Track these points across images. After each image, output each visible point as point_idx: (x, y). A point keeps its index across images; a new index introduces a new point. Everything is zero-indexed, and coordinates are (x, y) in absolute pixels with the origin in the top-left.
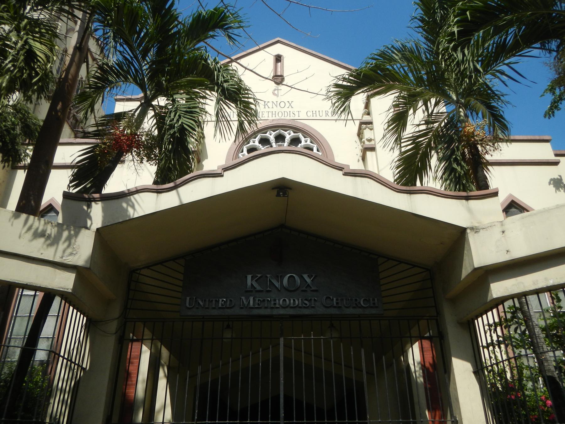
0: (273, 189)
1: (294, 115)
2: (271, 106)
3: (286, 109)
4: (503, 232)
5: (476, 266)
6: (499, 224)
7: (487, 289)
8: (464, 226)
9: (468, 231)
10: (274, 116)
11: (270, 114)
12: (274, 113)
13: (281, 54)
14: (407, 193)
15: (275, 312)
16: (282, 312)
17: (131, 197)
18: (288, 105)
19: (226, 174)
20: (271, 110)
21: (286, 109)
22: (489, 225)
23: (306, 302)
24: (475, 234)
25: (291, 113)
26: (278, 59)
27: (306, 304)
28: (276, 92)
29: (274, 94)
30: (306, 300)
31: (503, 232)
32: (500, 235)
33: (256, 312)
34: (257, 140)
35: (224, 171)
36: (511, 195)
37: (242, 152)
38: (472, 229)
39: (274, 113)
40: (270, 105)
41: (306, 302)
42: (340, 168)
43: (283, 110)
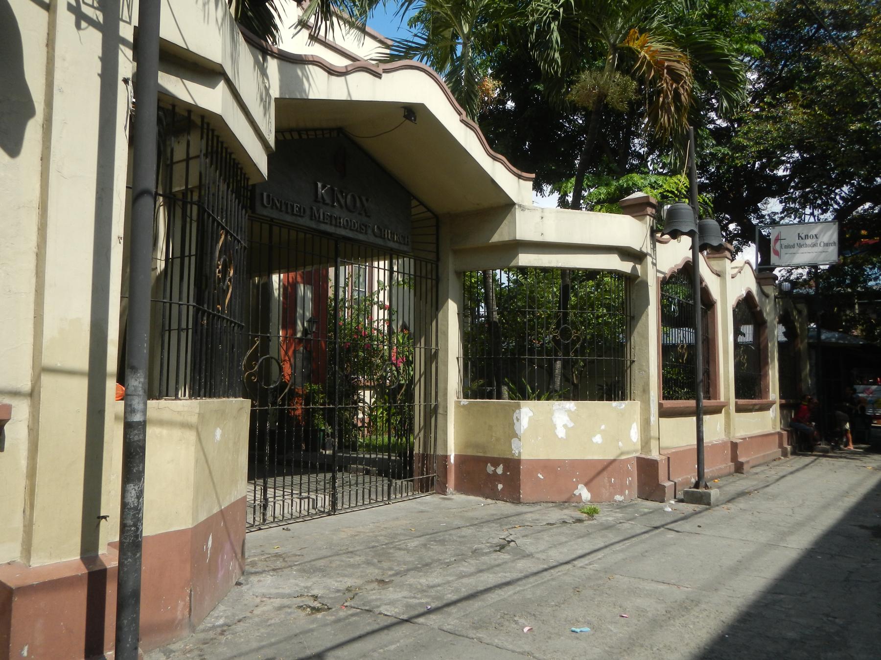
0: (403, 107)
4: (542, 218)
5: (518, 237)
6: (540, 211)
7: (515, 256)
8: (515, 202)
9: (517, 207)
14: (493, 158)
17: (306, 66)
19: (384, 75)
22: (533, 208)
23: (363, 227)
24: (522, 212)
27: (363, 230)
30: (363, 225)
31: (542, 218)
32: (539, 219)
35: (383, 72)
38: (520, 206)
41: (363, 227)
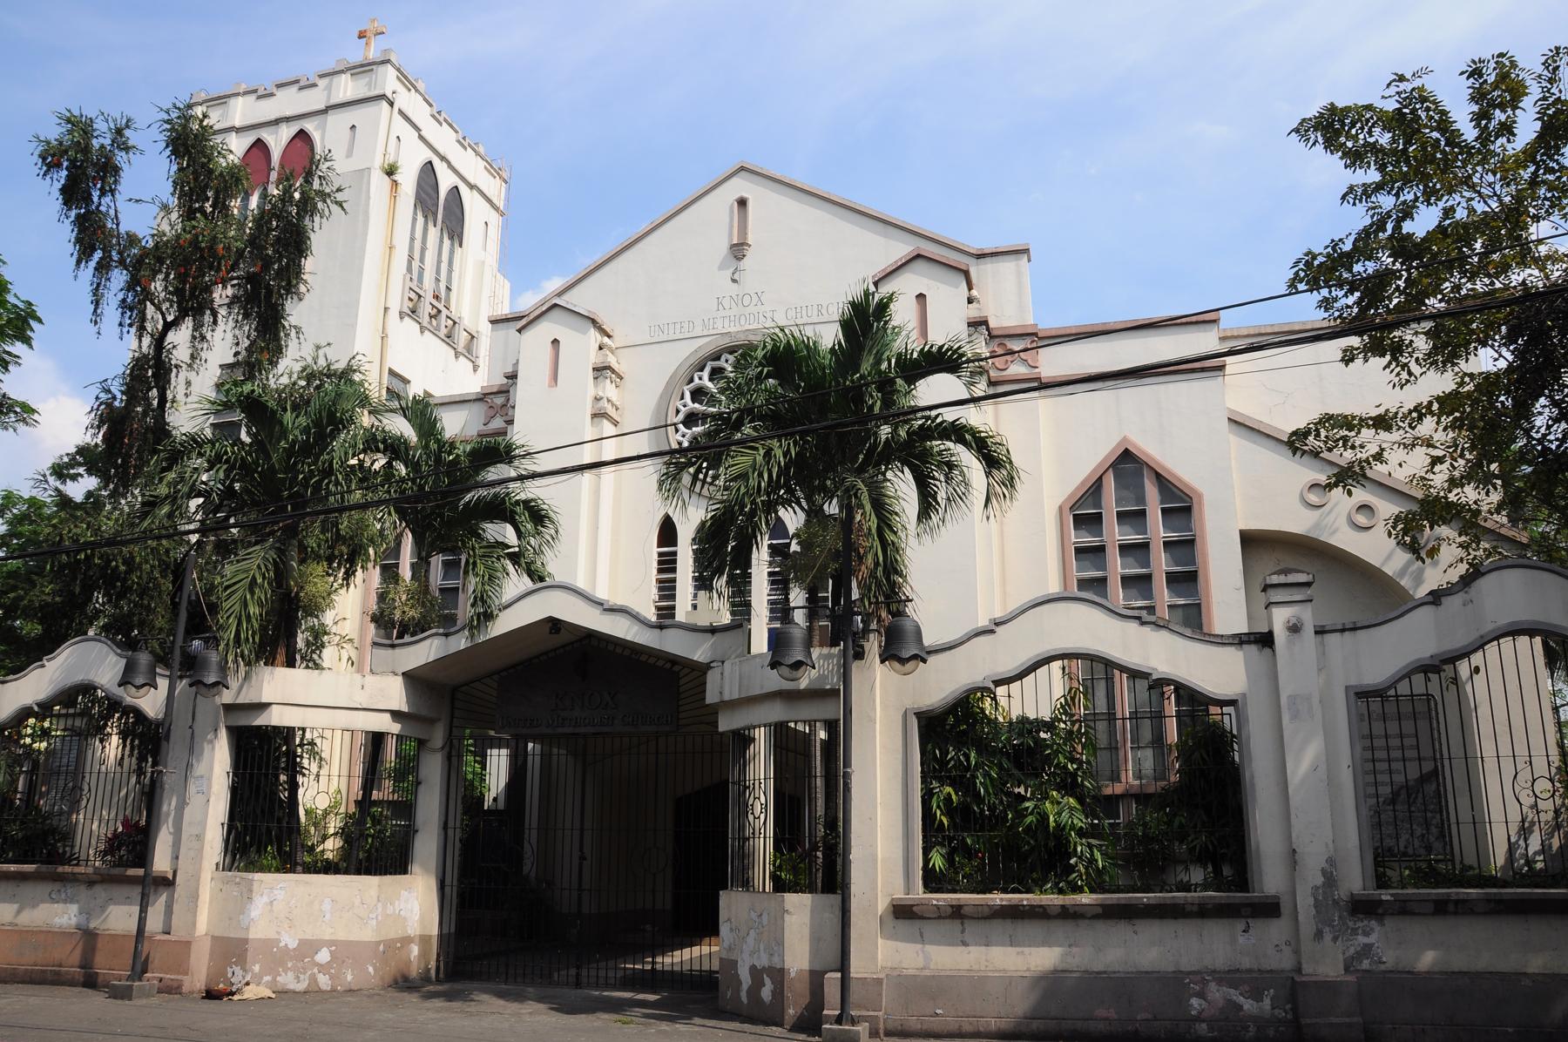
1: (764, 320)
2: (727, 307)
3: (752, 309)
10: (732, 324)
11: (727, 320)
12: (732, 318)
13: (745, 195)
15: (577, 730)
16: (582, 730)
18: (755, 298)
20: (727, 313)
21: (752, 309)
25: (761, 315)
26: (742, 203)
28: (736, 277)
29: (734, 281)
33: (560, 730)
34: (706, 374)
36: (1125, 439)
37: (682, 398)
39: (732, 318)
40: (726, 303)
42: (599, 603)
43: (748, 310)
